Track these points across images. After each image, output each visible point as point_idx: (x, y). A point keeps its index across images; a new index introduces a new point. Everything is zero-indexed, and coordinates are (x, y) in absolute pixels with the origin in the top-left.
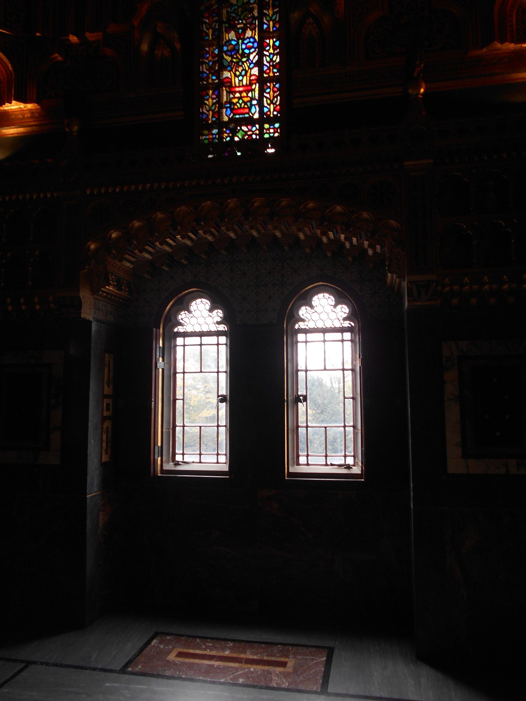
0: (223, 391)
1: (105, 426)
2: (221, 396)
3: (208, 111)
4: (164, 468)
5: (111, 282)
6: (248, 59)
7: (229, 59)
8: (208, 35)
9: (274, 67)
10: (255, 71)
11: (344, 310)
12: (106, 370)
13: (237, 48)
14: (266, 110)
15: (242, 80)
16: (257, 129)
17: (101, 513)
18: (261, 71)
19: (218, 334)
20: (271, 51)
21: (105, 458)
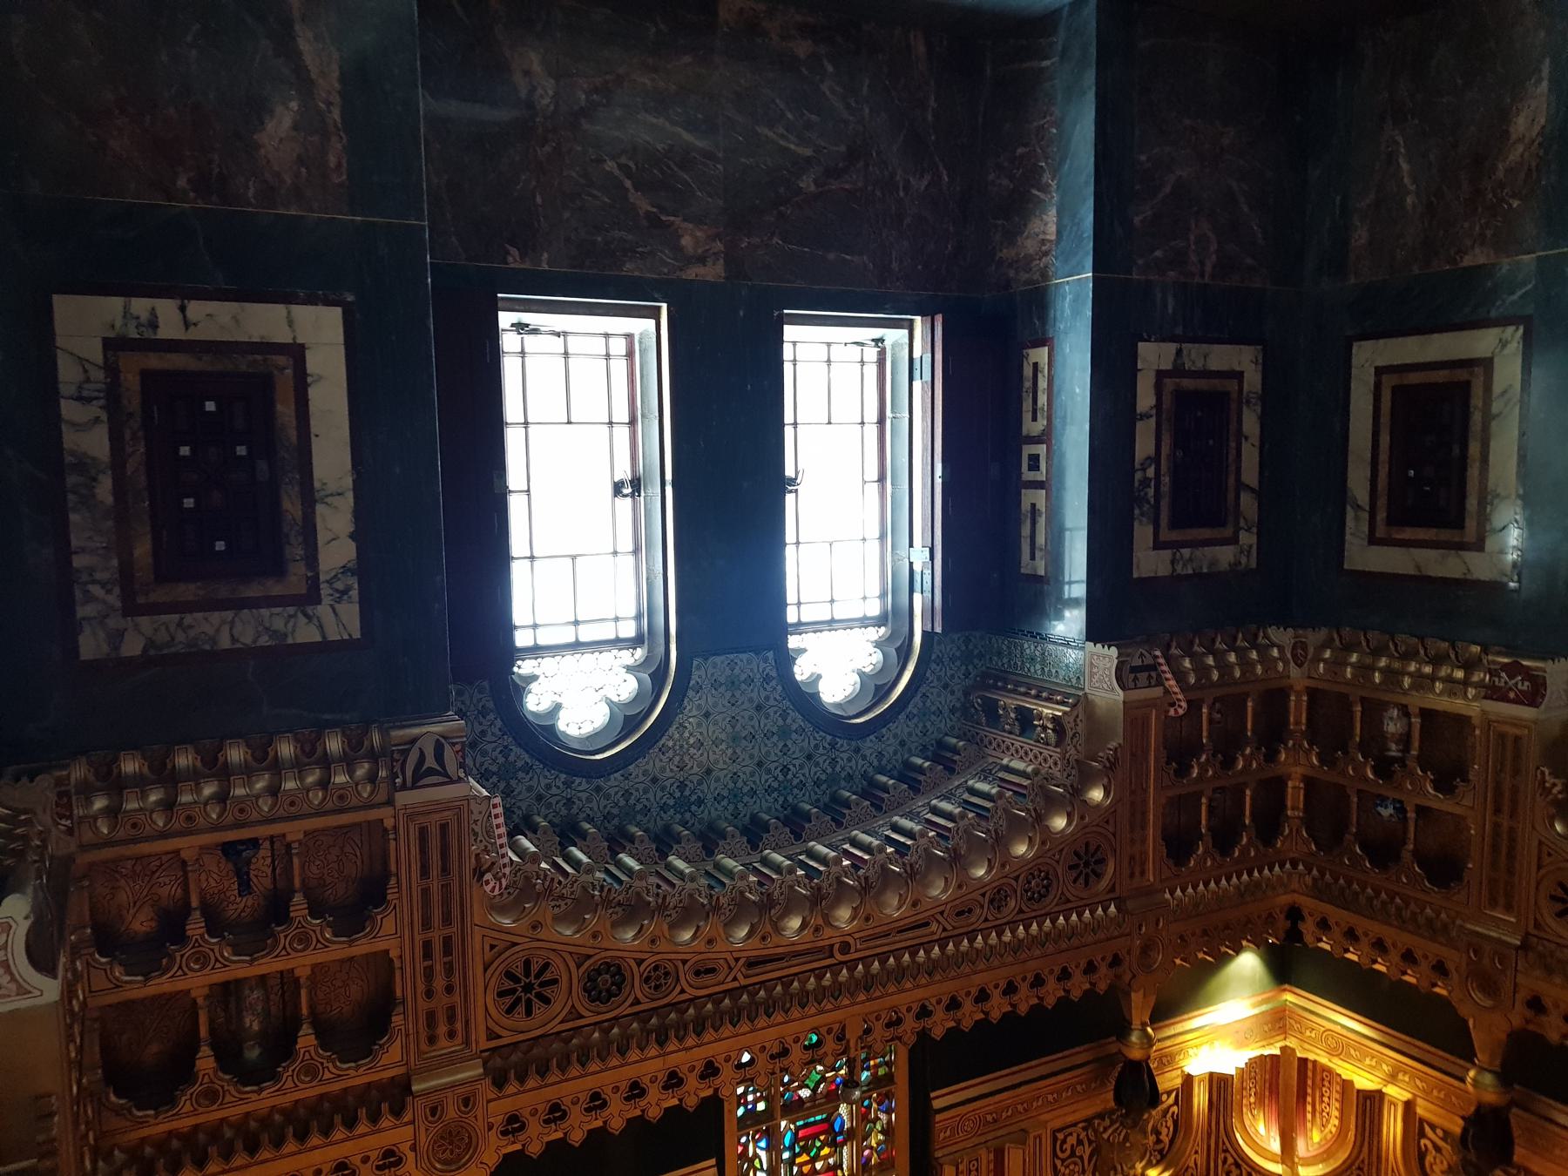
0: (790, 499)
1: (1042, 423)
2: (791, 492)
3: (878, 1119)
4: (905, 332)
5: (1050, 726)
11: (535, 702)
12: (1041, 539)
16: (783, 1096)
17: (1053, 237)
19: (800, 627)
21: (1041, 355)
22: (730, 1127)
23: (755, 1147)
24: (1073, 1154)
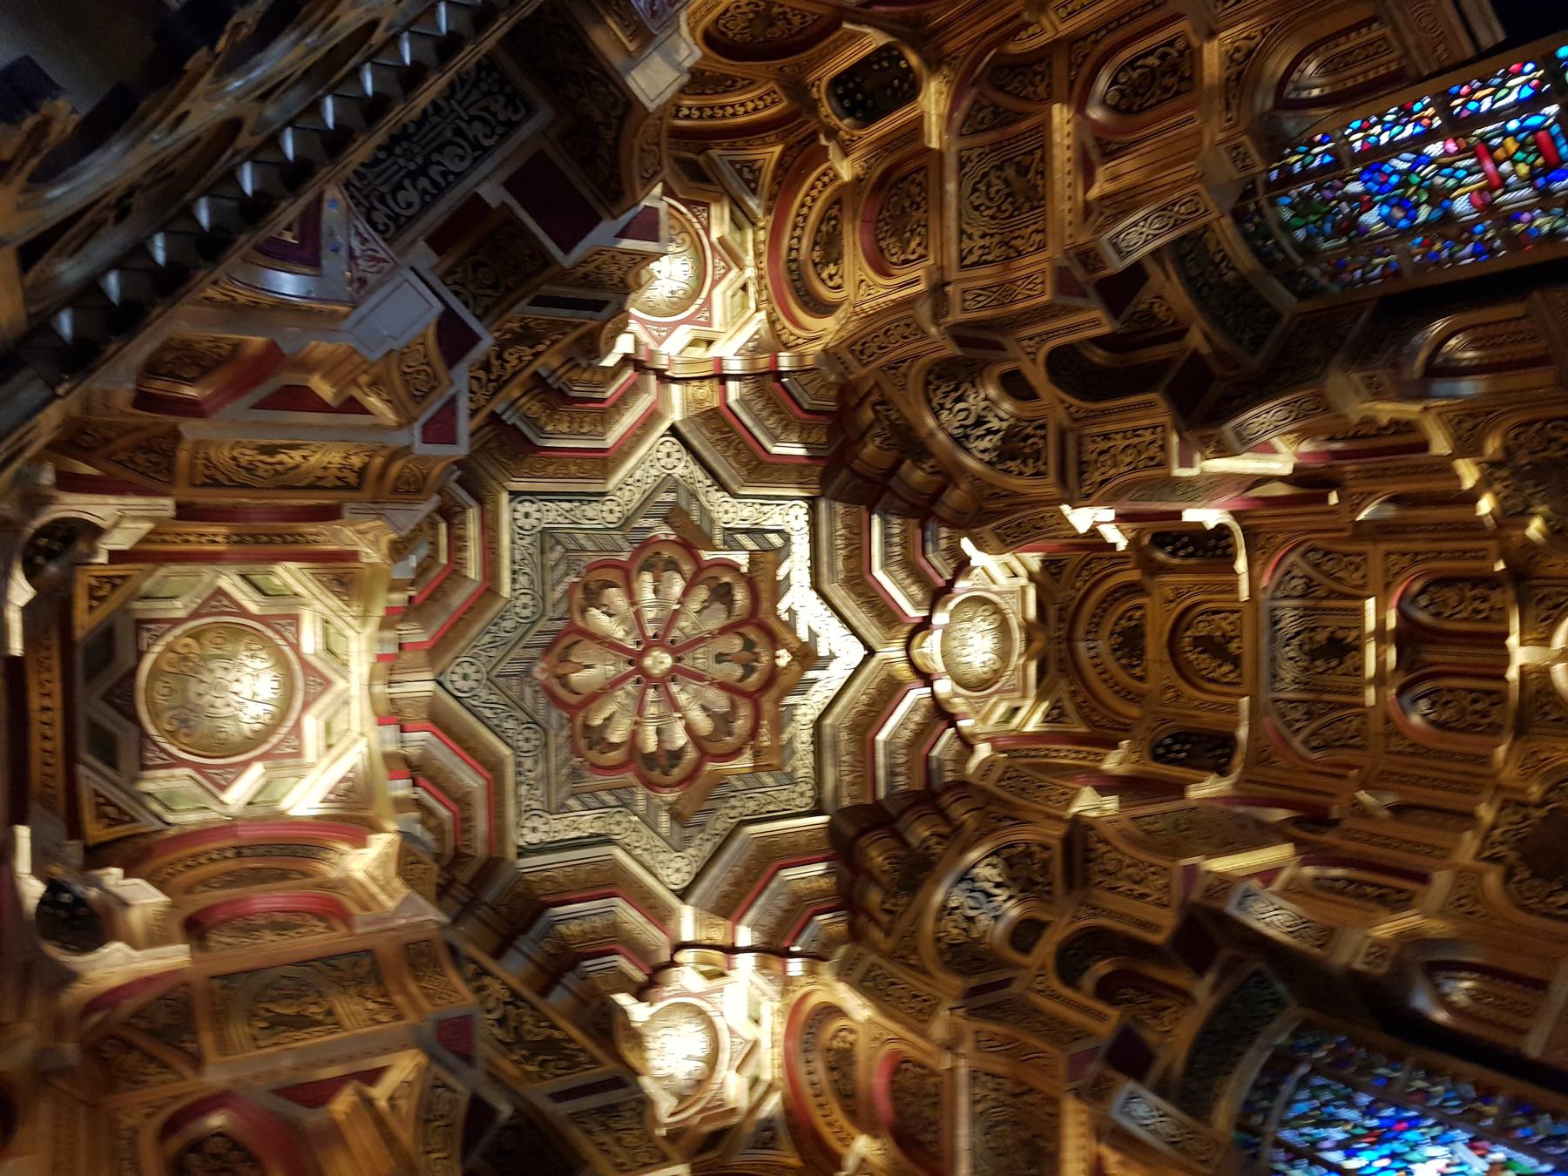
6: (1411, 170)
7: (1424, 213)
8: (1386, 265)
9: (1409, 113)
10: (1434, 149)
13: (1394, 201)
14: (1527, 92)
15: (1466, 168)
18: (1430, 136)
20: (1377, 129)
22: (1541, 45)
23: (1523, 85)
24: (1551, 440)
